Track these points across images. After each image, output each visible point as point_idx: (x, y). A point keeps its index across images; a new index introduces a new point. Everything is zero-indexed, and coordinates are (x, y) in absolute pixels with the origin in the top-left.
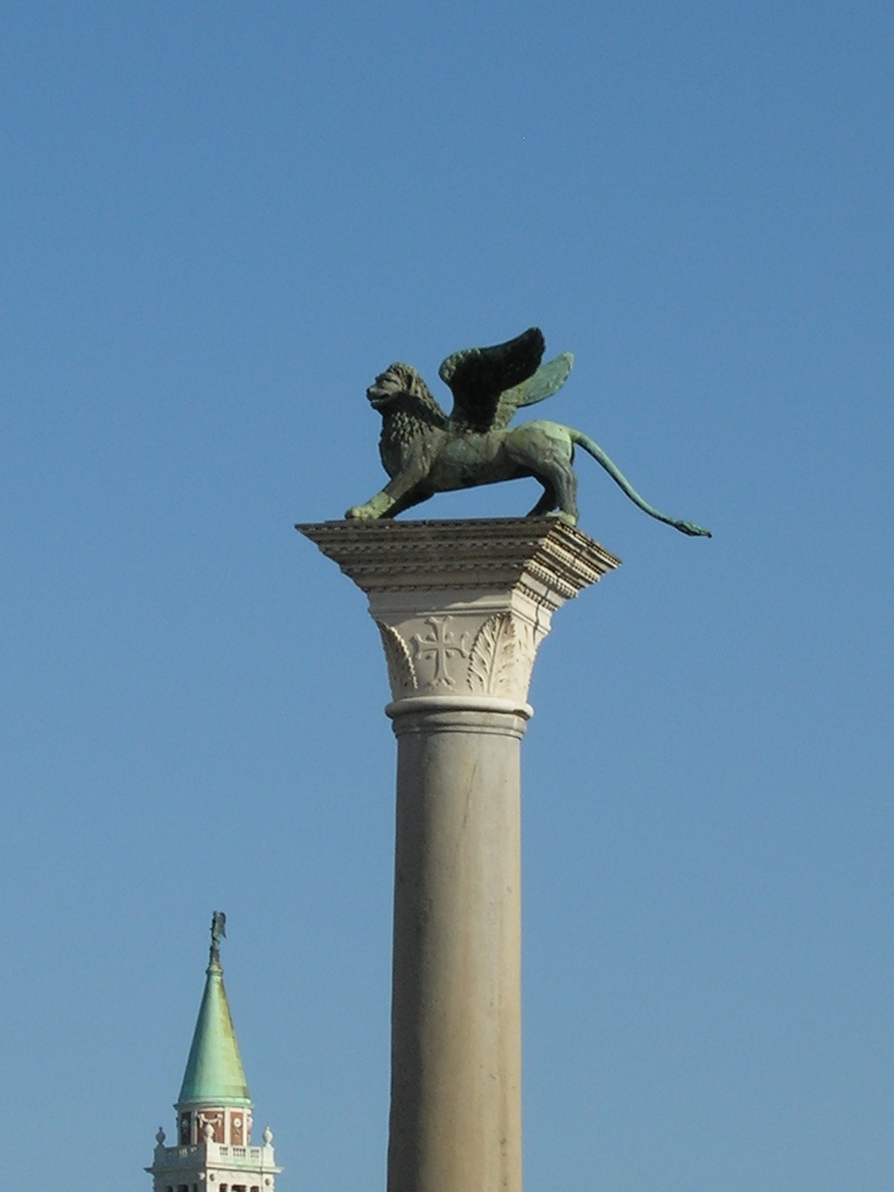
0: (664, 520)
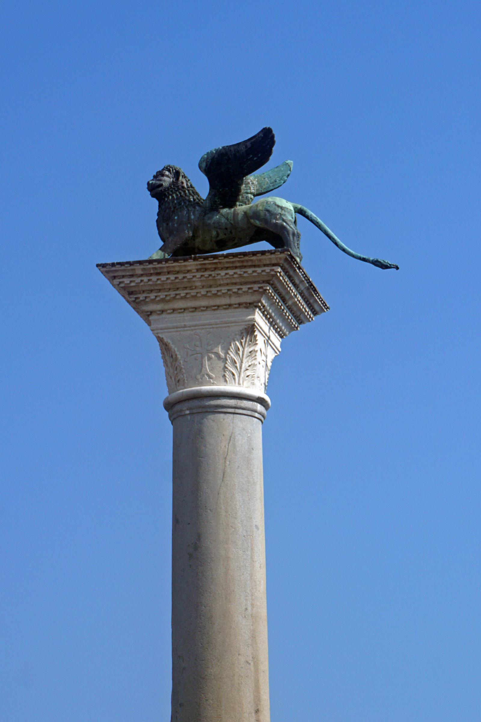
0: (364, 260)
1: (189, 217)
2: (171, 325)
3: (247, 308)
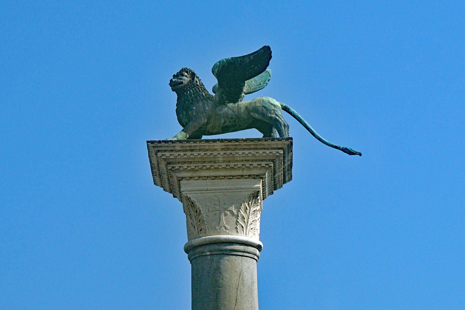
0: (336, 147)
1: (204, 108)
2: (196, 188)
3: (255, 178)
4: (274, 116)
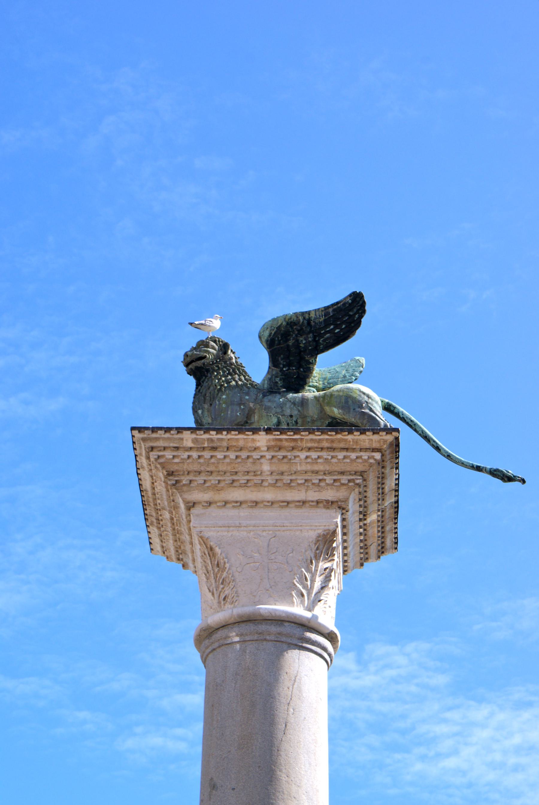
0: (478, 469)
4: (367, 411)
